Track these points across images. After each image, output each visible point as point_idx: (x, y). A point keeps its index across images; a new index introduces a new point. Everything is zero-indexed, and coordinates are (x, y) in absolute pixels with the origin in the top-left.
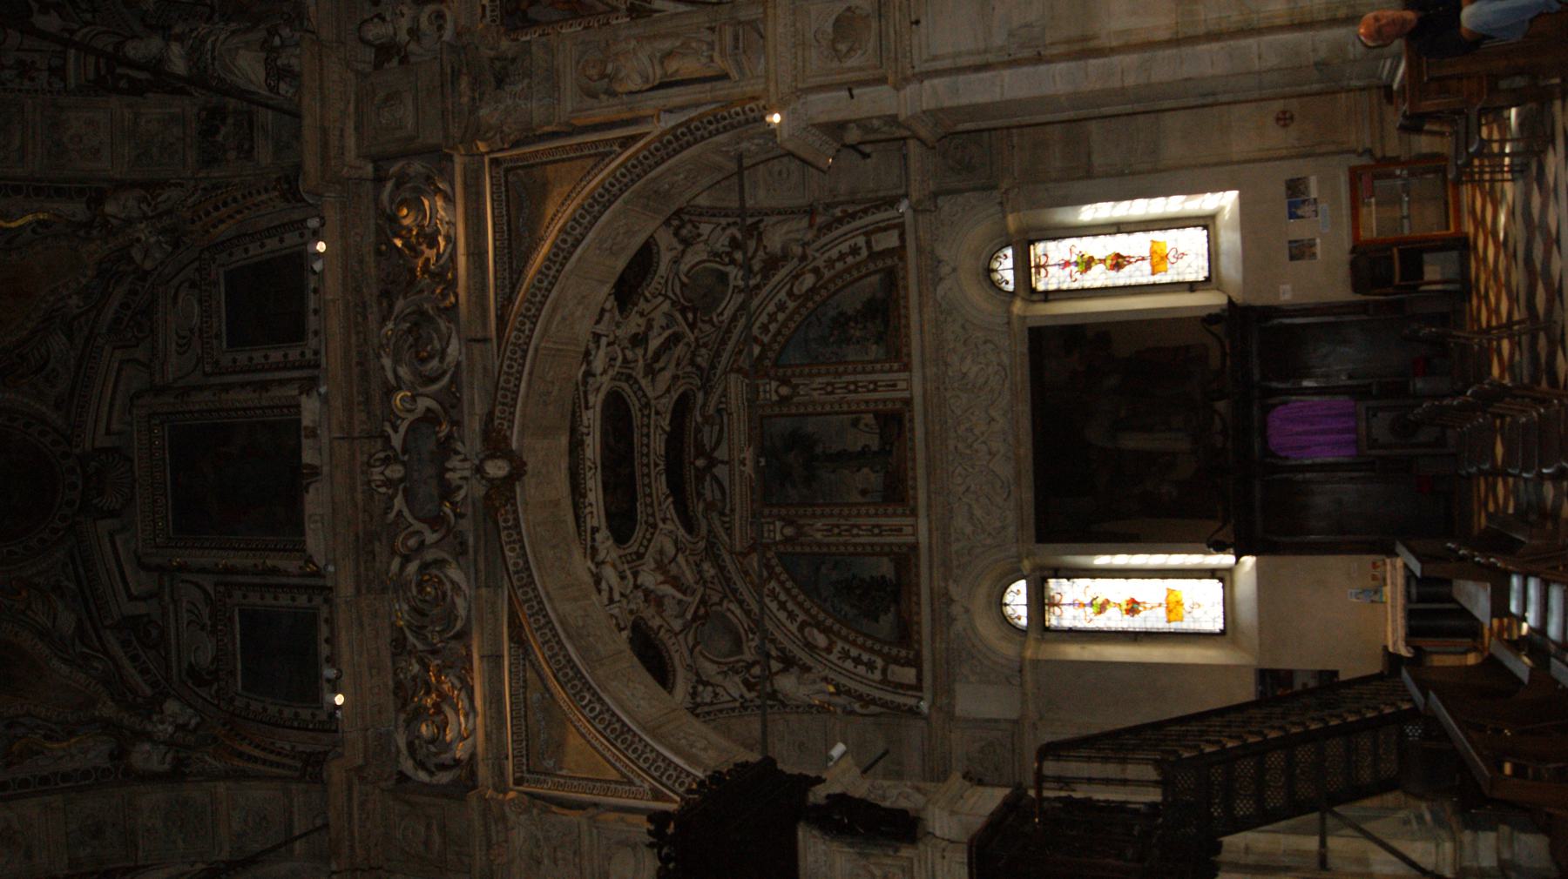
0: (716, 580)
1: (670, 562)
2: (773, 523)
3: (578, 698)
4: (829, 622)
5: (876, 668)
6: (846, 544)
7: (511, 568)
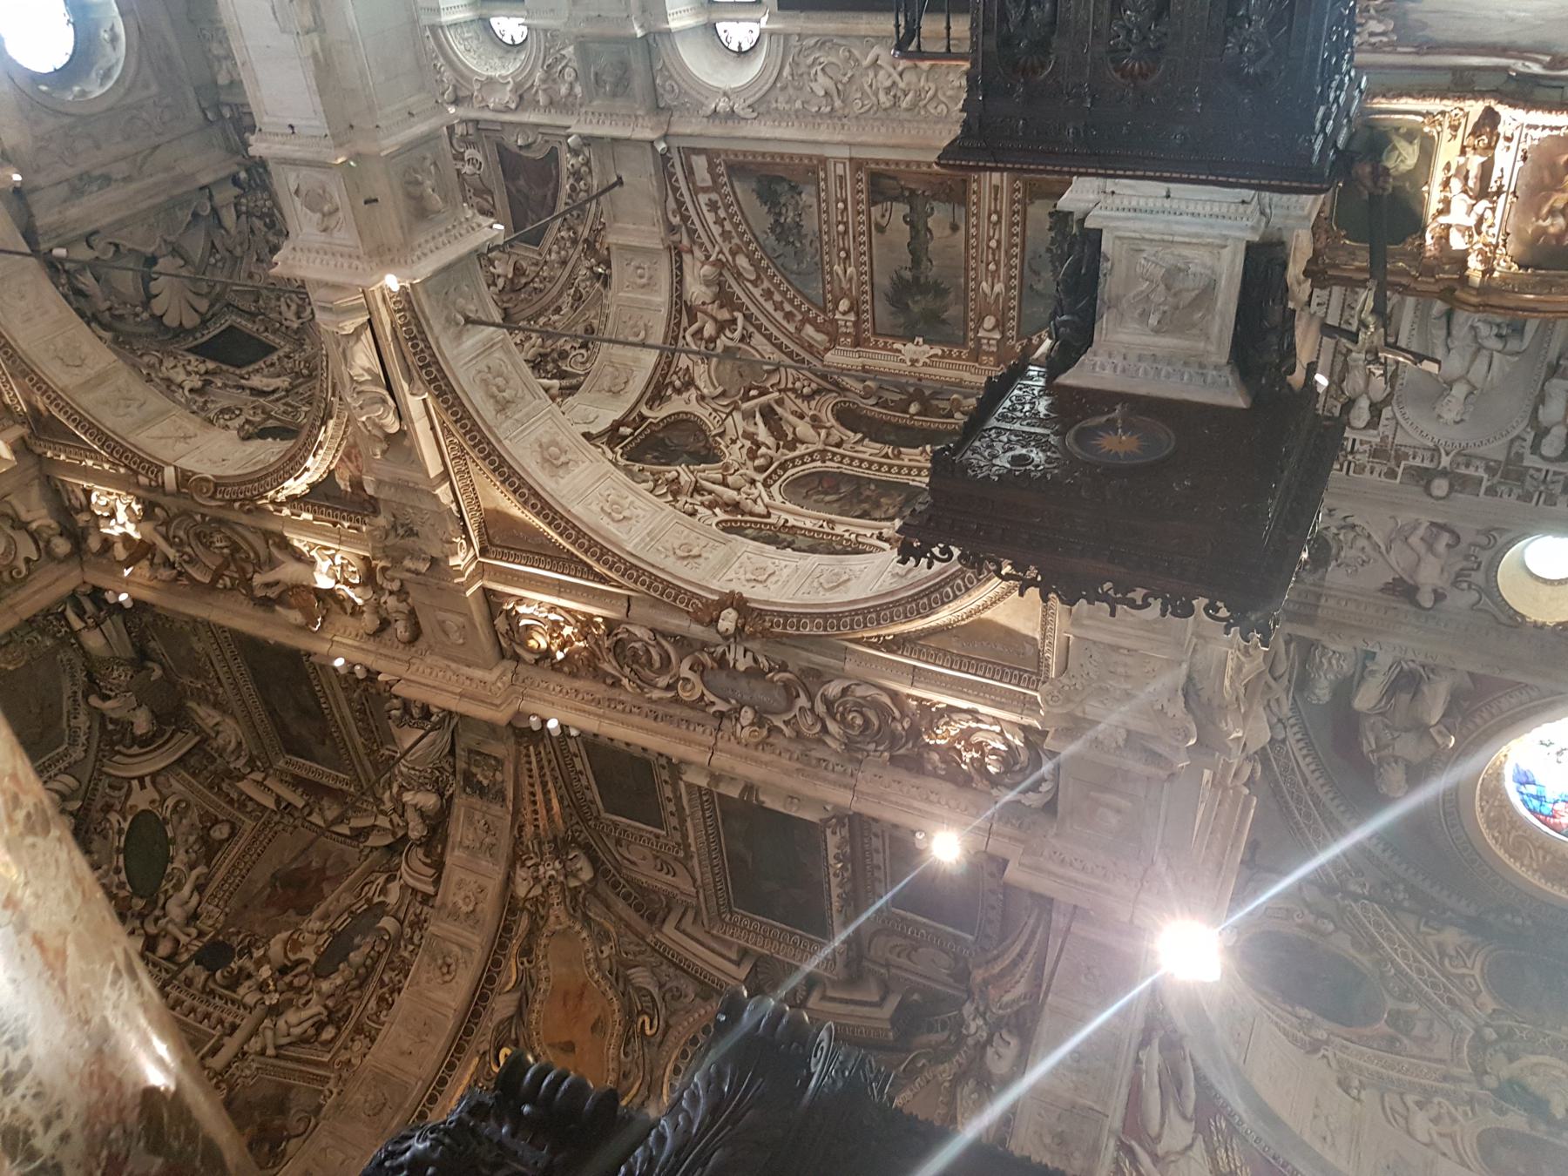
6: (1009, 256)
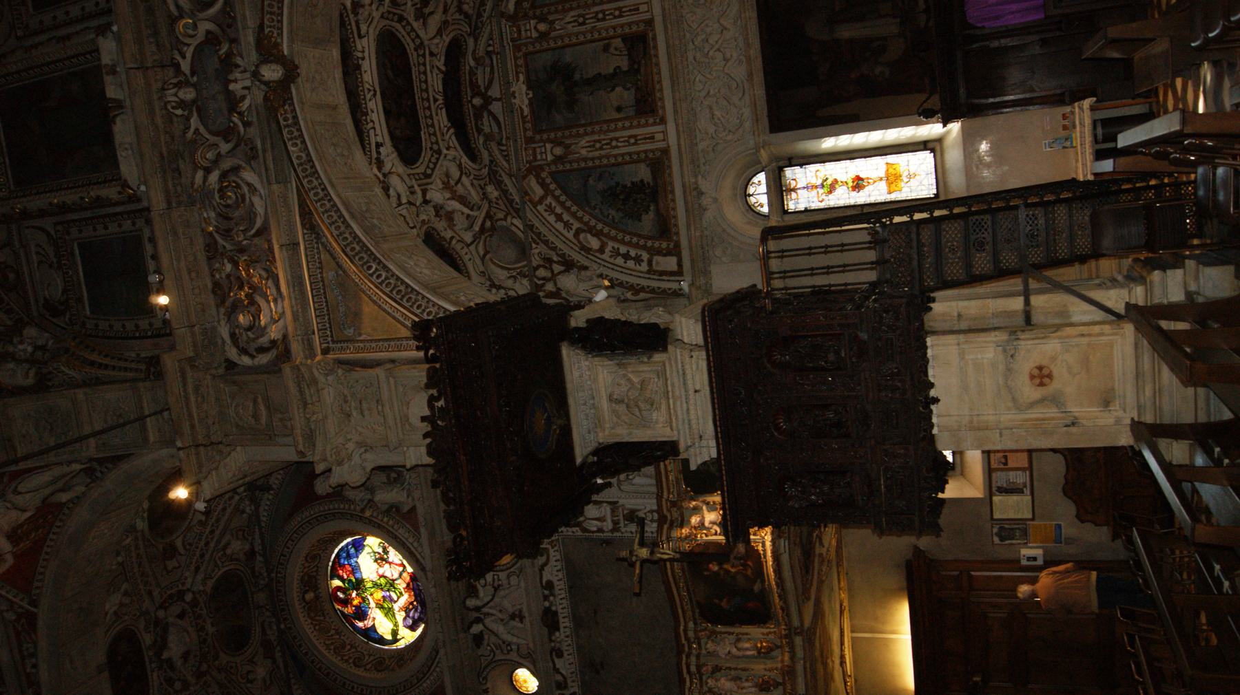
0: (500, 202)
1: (456, 184)
2: (545, 146)
3: (365, 267)
4: (600, 226)
5: (643, 261)
6: (607, 157)
7: (295, 162)
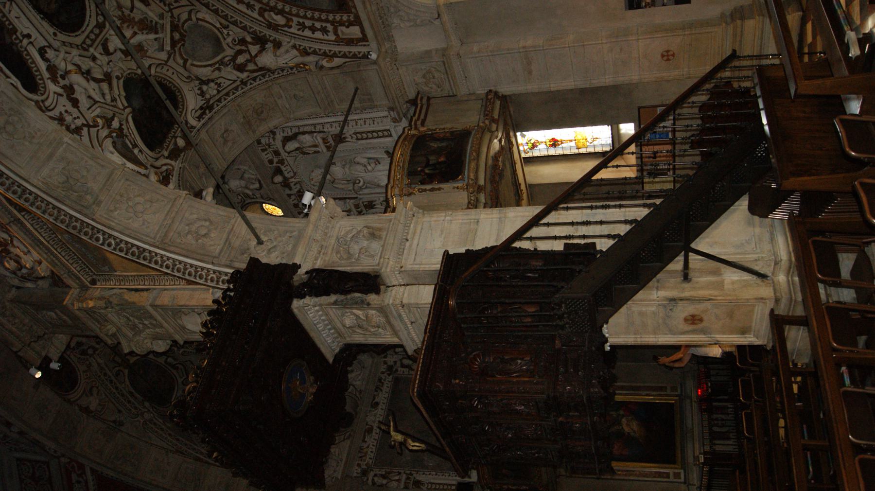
1: (132, 11)
